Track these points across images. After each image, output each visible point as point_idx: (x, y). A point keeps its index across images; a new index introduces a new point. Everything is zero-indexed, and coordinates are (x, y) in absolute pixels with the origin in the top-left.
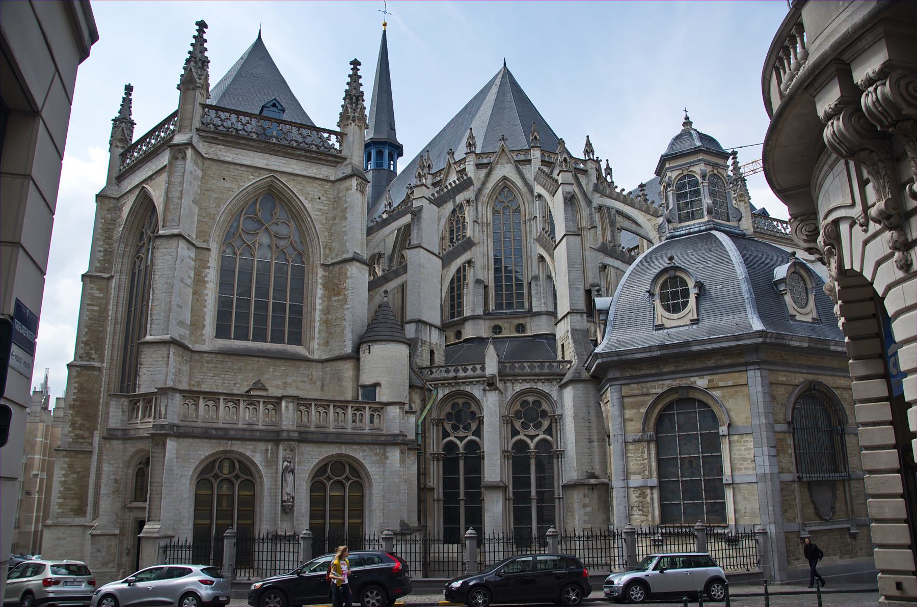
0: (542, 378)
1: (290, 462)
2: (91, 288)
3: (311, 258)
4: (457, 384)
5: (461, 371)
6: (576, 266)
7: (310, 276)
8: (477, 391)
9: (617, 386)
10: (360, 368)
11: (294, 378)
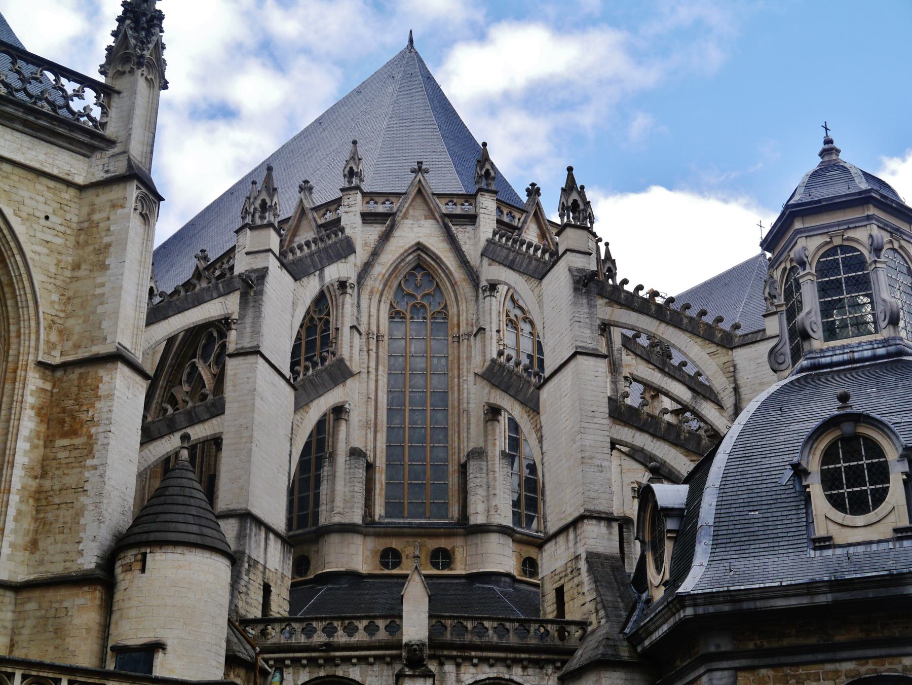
0: (523, 656)
4: (330, 661)
5: (340, 632)
6: (596, 420)
9: (726, 673)
10: (115, 608)
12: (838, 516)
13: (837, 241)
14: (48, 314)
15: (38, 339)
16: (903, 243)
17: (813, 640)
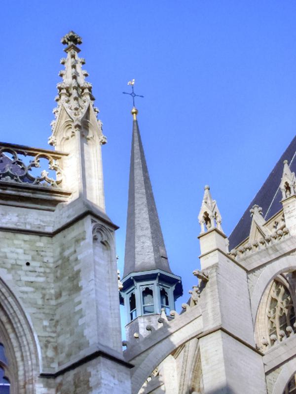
14: (42, 337)
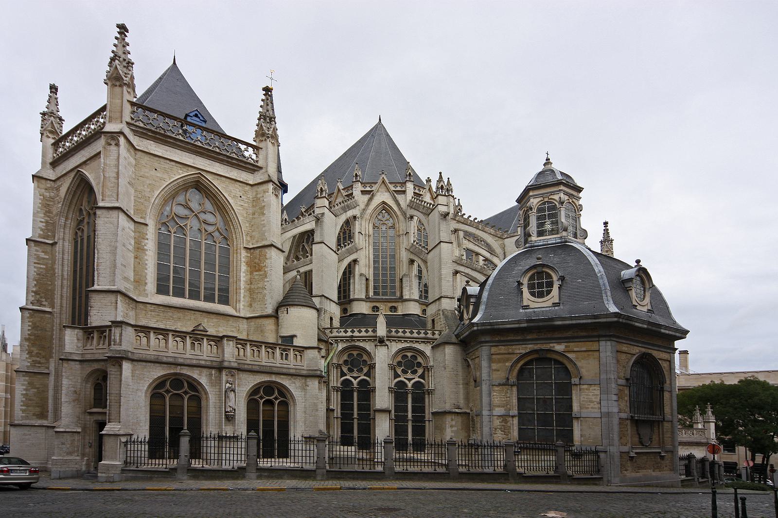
1: (232, 384)
2: (36, 250)
3: (235, 242)
5: (356, 332)
7: (235, 255)
8: (368, 346)
11: (225, 328)
12: (533, 298)
13: (546, 200)
15: (243, 239)
16: (574, 200)
17: (519, 338)
